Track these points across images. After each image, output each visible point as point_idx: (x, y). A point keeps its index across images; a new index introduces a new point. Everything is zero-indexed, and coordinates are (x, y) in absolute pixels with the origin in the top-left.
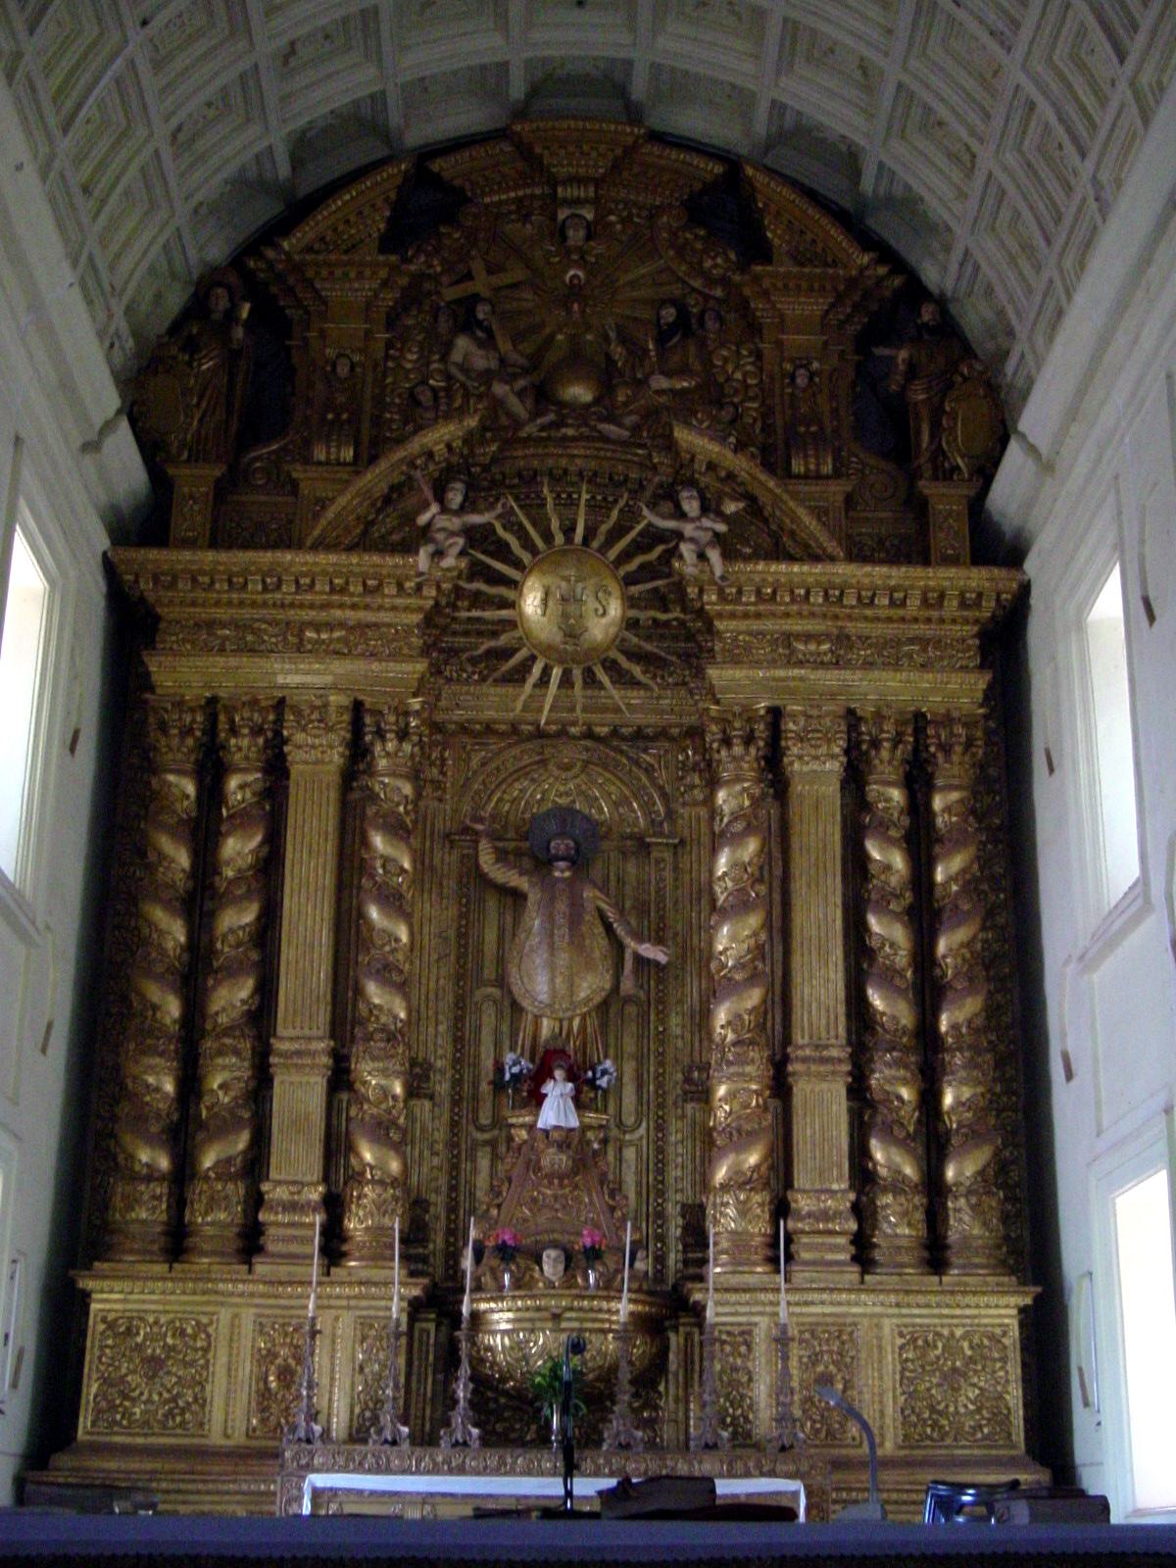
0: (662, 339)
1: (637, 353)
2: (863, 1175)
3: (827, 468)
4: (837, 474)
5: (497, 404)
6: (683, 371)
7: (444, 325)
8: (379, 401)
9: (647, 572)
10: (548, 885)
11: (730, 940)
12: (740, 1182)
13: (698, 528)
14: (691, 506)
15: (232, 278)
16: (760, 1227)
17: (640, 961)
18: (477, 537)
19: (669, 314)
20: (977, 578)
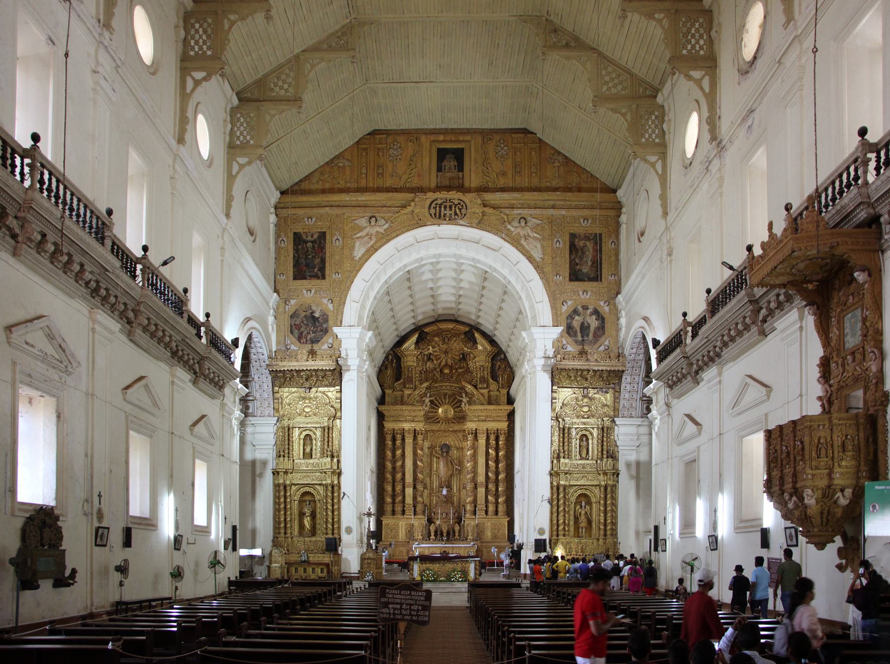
0: (460, 360)
1: (456, 364)
2: (487, 501)
3: (485, 386)
4: (487, 387)
5: (434, 375)
6: (464, 367)
7: (425, 358)
8: (416, 374)
9: (457, 407)
10: (442, 455)
11: (469, 465)
12: (470, 503)
13: (465, 400)
14: (464, 396)
15: (391, 352)
16: (473, 509)
17: (456, 469)
18: (431, 401)
19: (461, 356)
20: (510, 408)
